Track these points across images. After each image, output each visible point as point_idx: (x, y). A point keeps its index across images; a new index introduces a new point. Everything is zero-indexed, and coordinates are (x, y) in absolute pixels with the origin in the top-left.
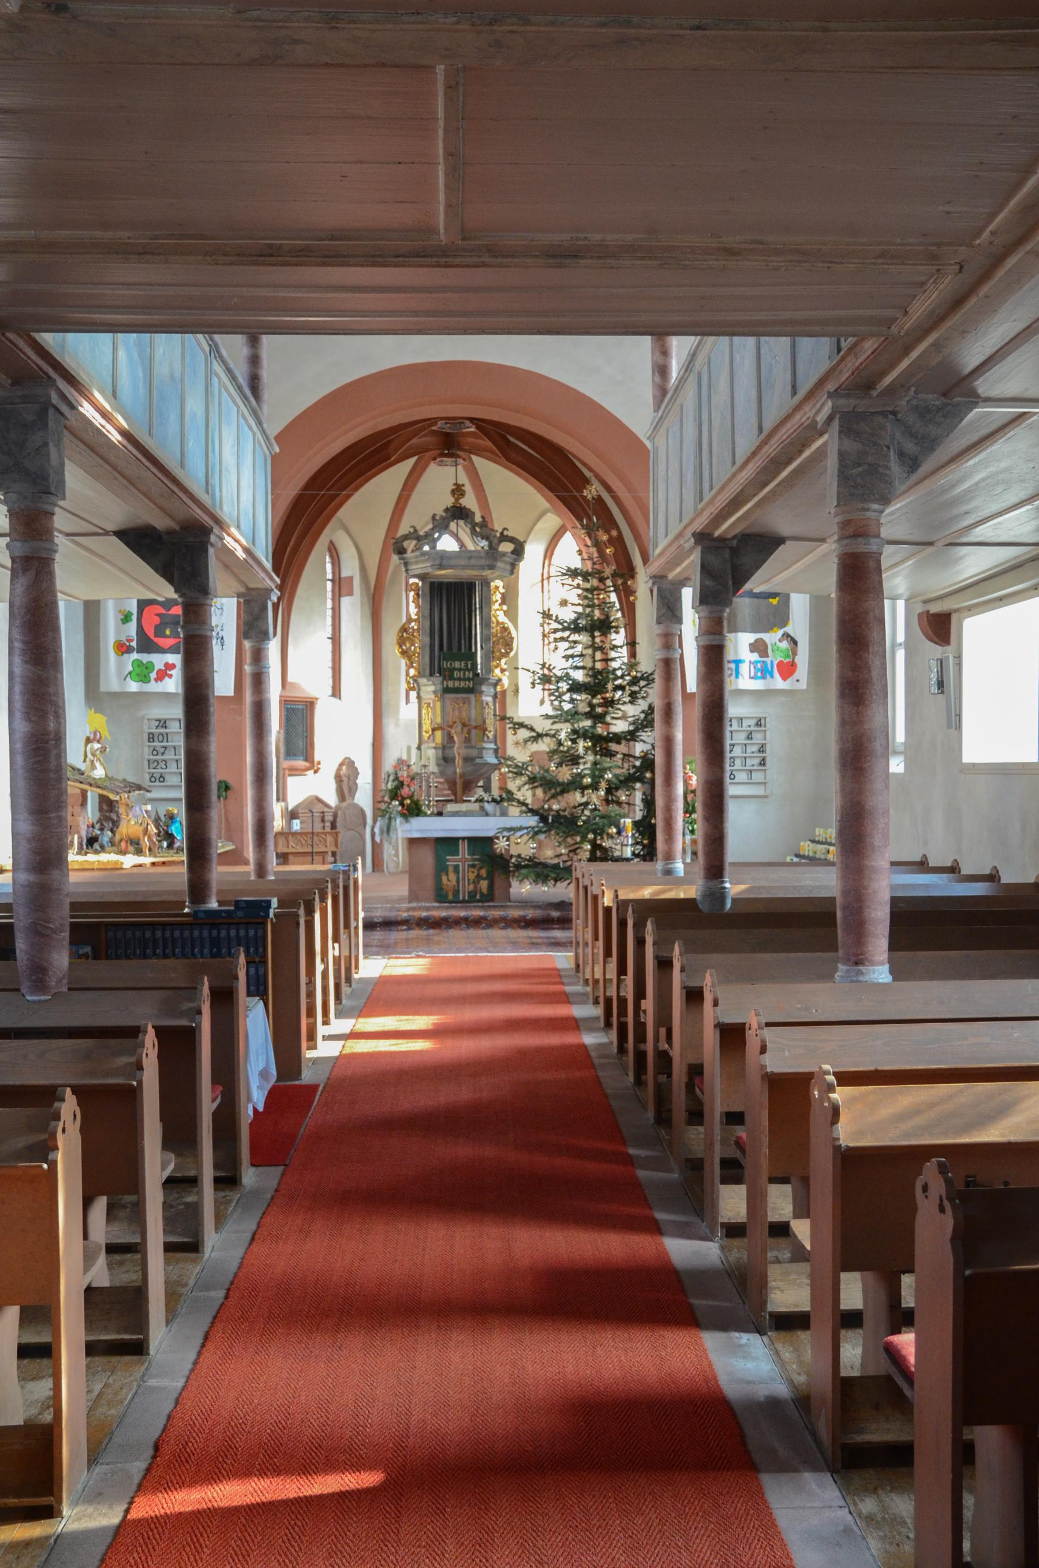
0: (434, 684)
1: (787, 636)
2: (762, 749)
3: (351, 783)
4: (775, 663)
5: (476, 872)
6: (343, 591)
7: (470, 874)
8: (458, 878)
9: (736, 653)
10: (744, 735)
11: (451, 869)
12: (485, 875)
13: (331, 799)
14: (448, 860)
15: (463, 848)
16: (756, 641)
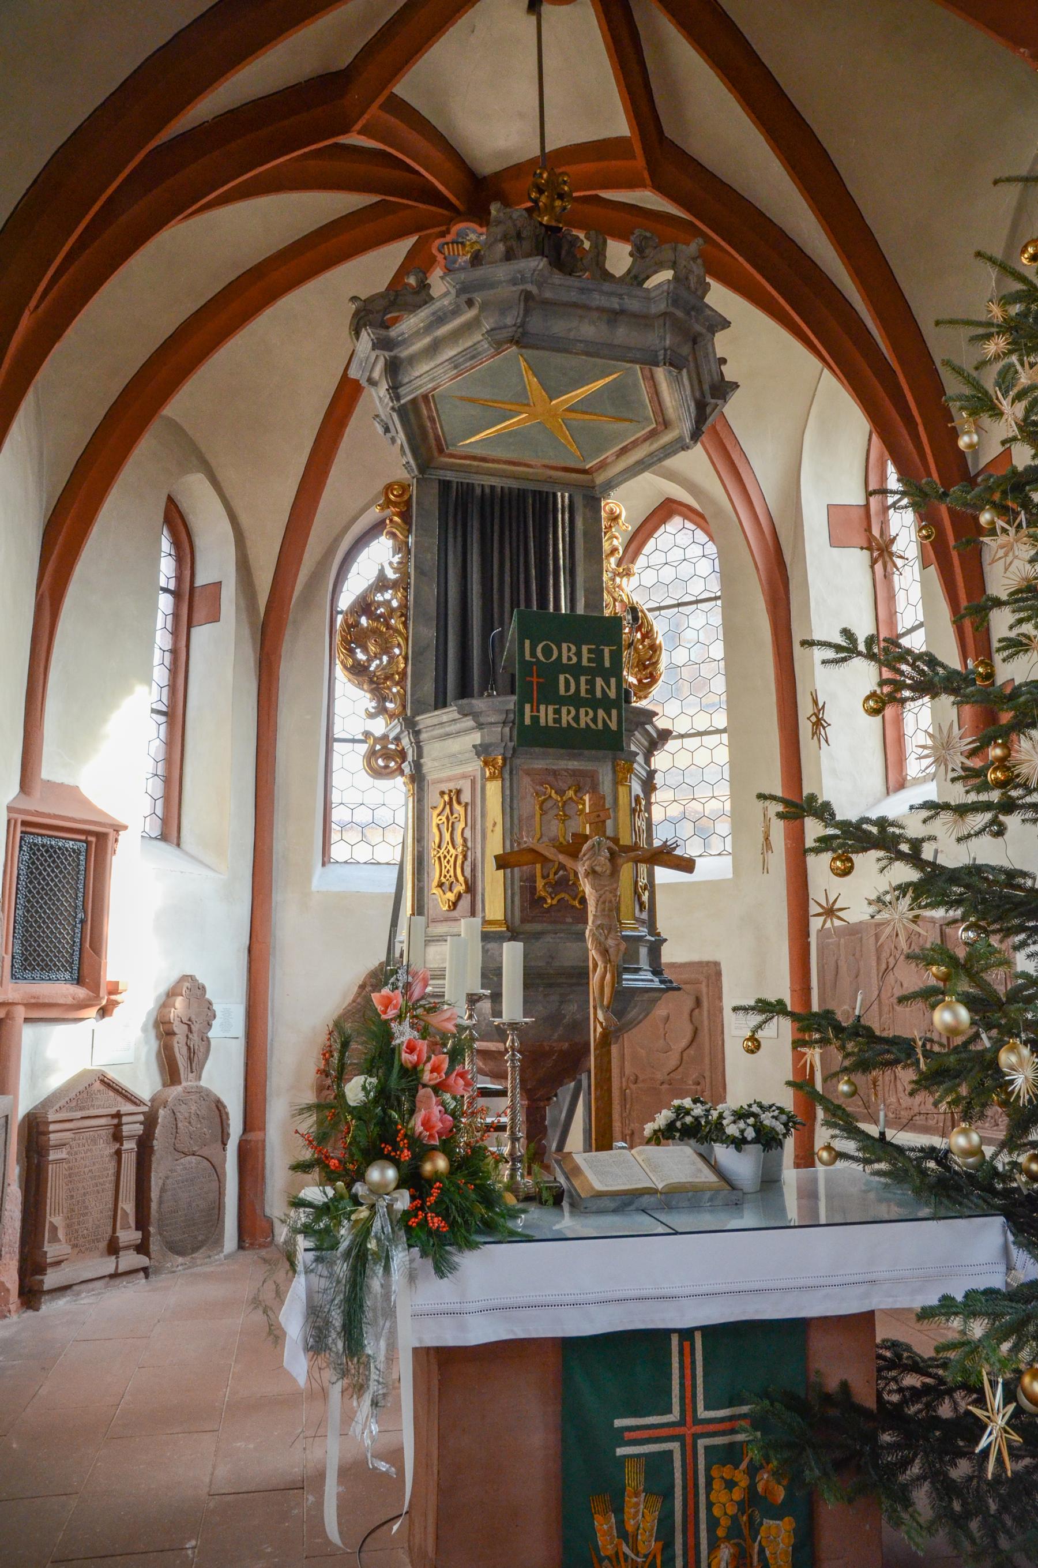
0: (480, 726)
3: (195, 1038)
5: (744, 1482)
6: (197, 616)
7: (720, 1495)
8: (665, 1522)
11: (633, 1479)
12: (780, 1494)
13: (144, 1083)
14: (620, 1437)
15: (687, 1377)
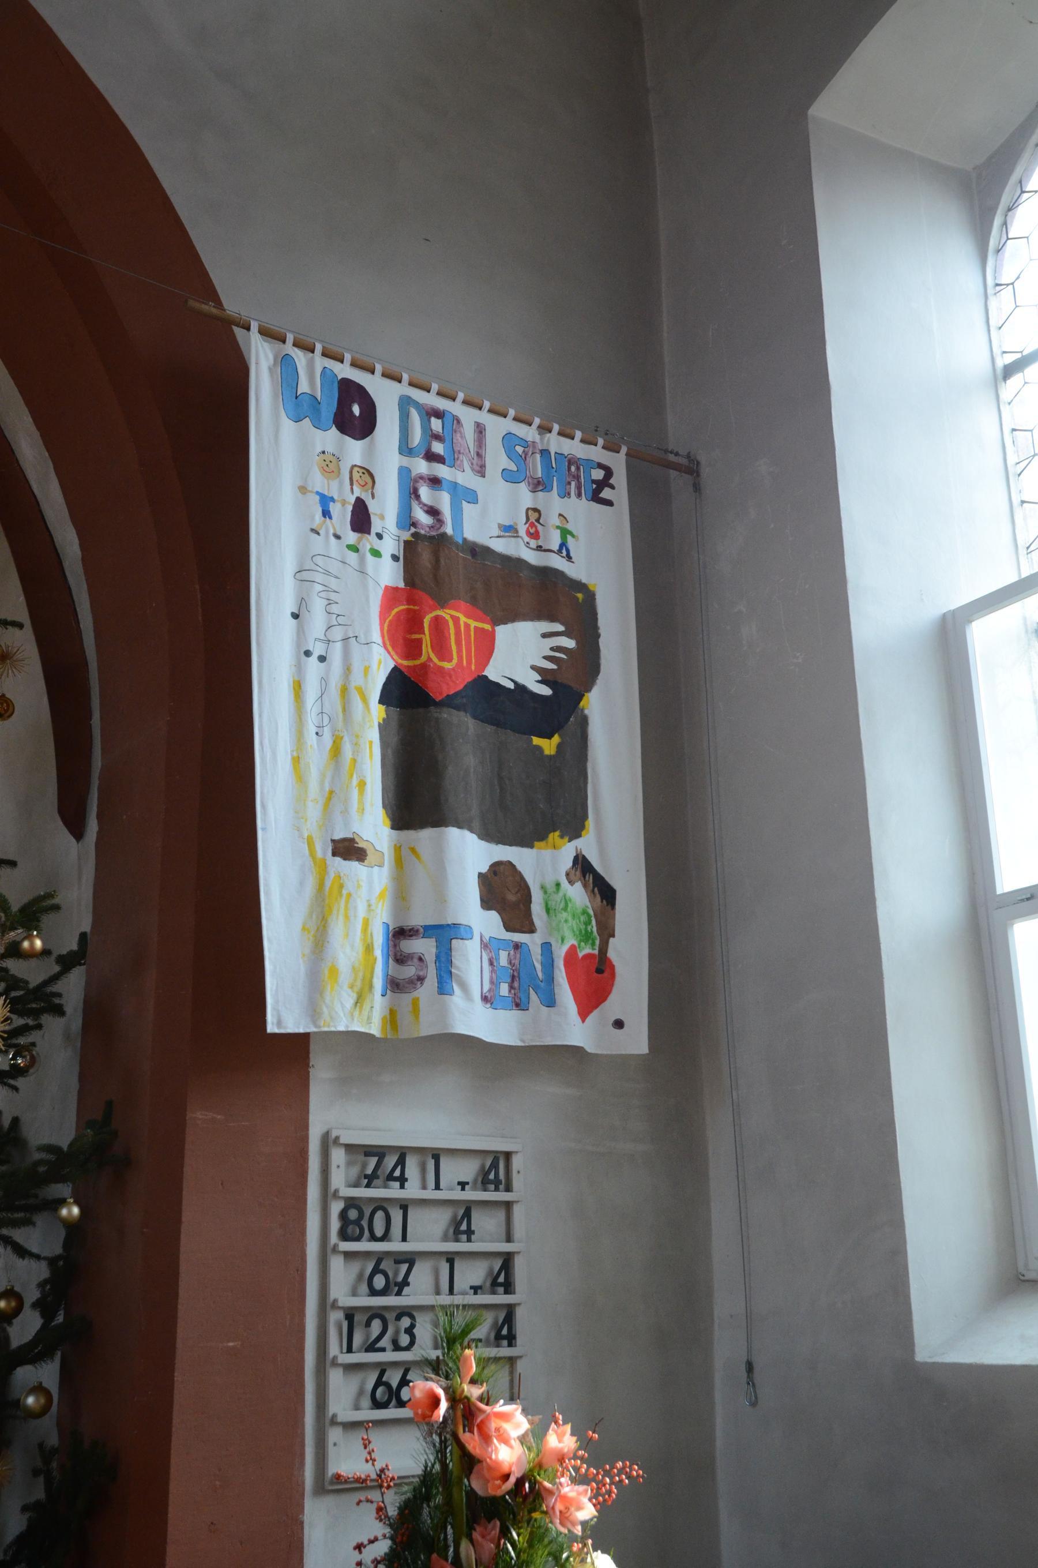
1: (582, 866)
2: (503, 1277)
4: (560, 952)
9: (441, 896)
10: (442, 1219)
16: (497, 868)
